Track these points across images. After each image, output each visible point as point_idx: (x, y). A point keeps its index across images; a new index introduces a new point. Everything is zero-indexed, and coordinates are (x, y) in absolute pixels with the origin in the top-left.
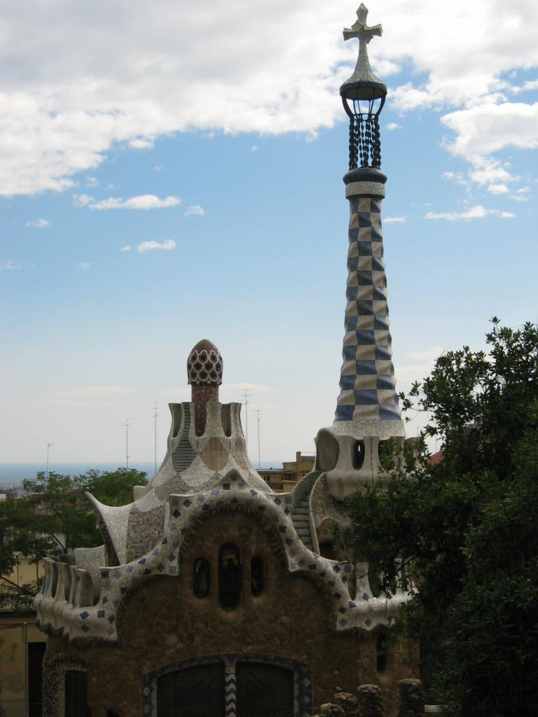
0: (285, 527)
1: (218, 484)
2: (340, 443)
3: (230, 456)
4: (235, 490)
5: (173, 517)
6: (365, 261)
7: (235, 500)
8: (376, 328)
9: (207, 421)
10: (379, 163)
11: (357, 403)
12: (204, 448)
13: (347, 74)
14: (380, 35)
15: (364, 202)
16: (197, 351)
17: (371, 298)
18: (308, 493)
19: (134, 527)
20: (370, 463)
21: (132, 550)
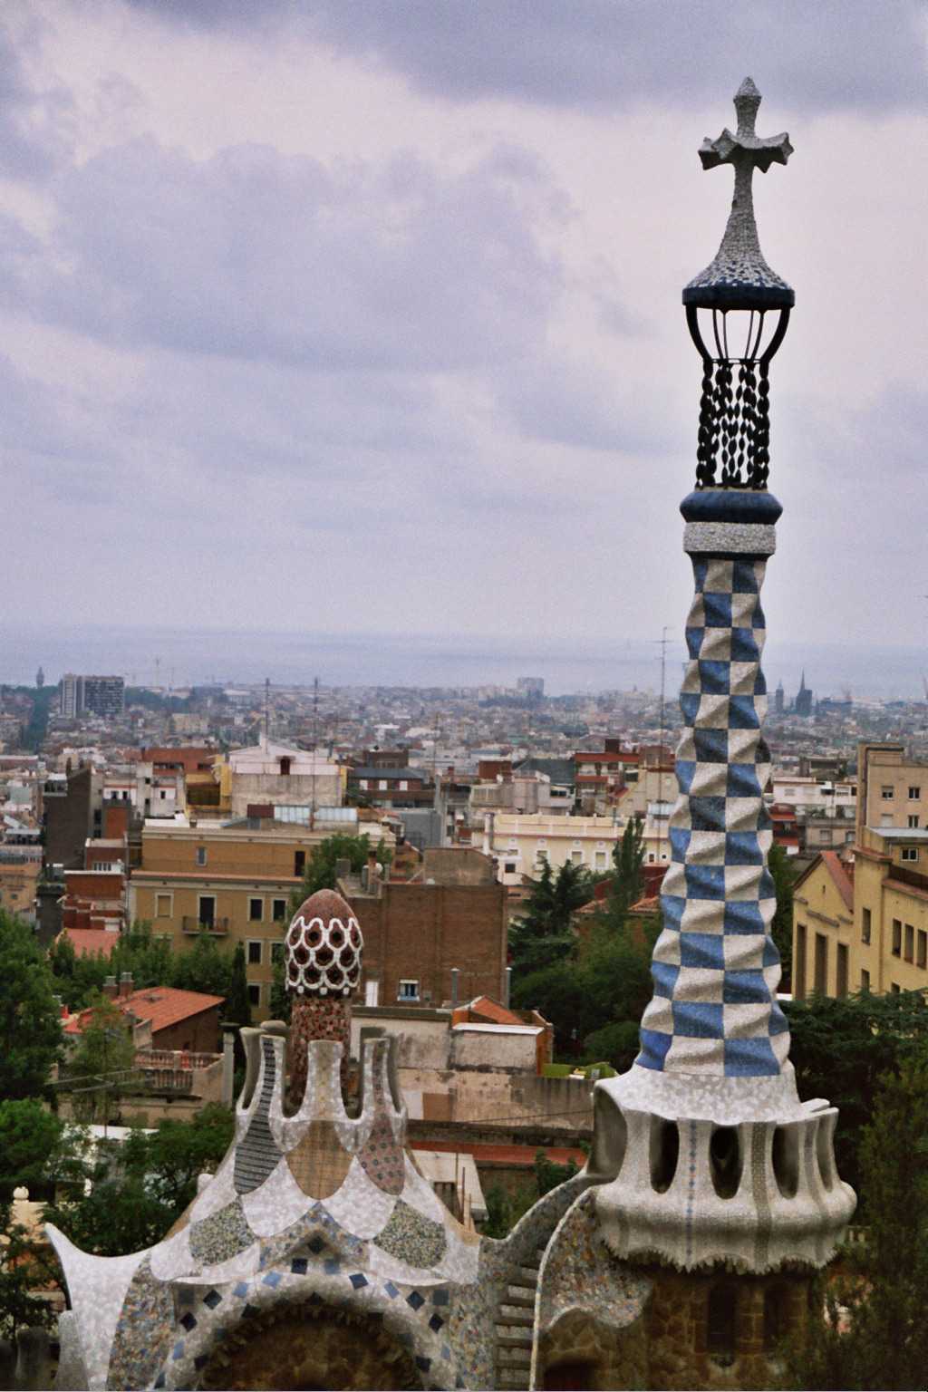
0: (429, 1361)
1: (283, 1258)
2: (628, 1120)
3: (355, 1163)
4: (316, 1276)
5: (181, 1327)
6: (712, 709)
7: (314, 1298)
8: (729, 862)
9: (309, 1082)
10: (765, 473)
11: (677, 1033)
12: (296, 1144)
13: (698, 257)
14: (784, 162)
15: (716, 570)
16: (302, 918)
17: (722, 792)
18: (542, 1246)
19: (133, 1318)
20: (687, 1179)
21: (122, 1372)
